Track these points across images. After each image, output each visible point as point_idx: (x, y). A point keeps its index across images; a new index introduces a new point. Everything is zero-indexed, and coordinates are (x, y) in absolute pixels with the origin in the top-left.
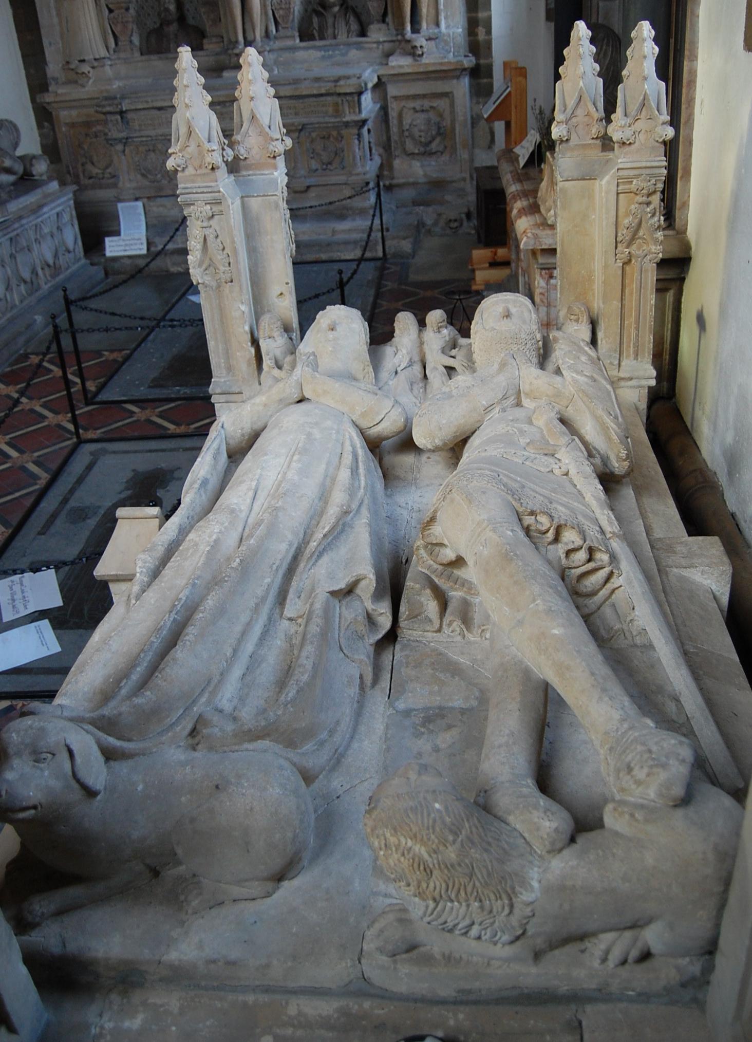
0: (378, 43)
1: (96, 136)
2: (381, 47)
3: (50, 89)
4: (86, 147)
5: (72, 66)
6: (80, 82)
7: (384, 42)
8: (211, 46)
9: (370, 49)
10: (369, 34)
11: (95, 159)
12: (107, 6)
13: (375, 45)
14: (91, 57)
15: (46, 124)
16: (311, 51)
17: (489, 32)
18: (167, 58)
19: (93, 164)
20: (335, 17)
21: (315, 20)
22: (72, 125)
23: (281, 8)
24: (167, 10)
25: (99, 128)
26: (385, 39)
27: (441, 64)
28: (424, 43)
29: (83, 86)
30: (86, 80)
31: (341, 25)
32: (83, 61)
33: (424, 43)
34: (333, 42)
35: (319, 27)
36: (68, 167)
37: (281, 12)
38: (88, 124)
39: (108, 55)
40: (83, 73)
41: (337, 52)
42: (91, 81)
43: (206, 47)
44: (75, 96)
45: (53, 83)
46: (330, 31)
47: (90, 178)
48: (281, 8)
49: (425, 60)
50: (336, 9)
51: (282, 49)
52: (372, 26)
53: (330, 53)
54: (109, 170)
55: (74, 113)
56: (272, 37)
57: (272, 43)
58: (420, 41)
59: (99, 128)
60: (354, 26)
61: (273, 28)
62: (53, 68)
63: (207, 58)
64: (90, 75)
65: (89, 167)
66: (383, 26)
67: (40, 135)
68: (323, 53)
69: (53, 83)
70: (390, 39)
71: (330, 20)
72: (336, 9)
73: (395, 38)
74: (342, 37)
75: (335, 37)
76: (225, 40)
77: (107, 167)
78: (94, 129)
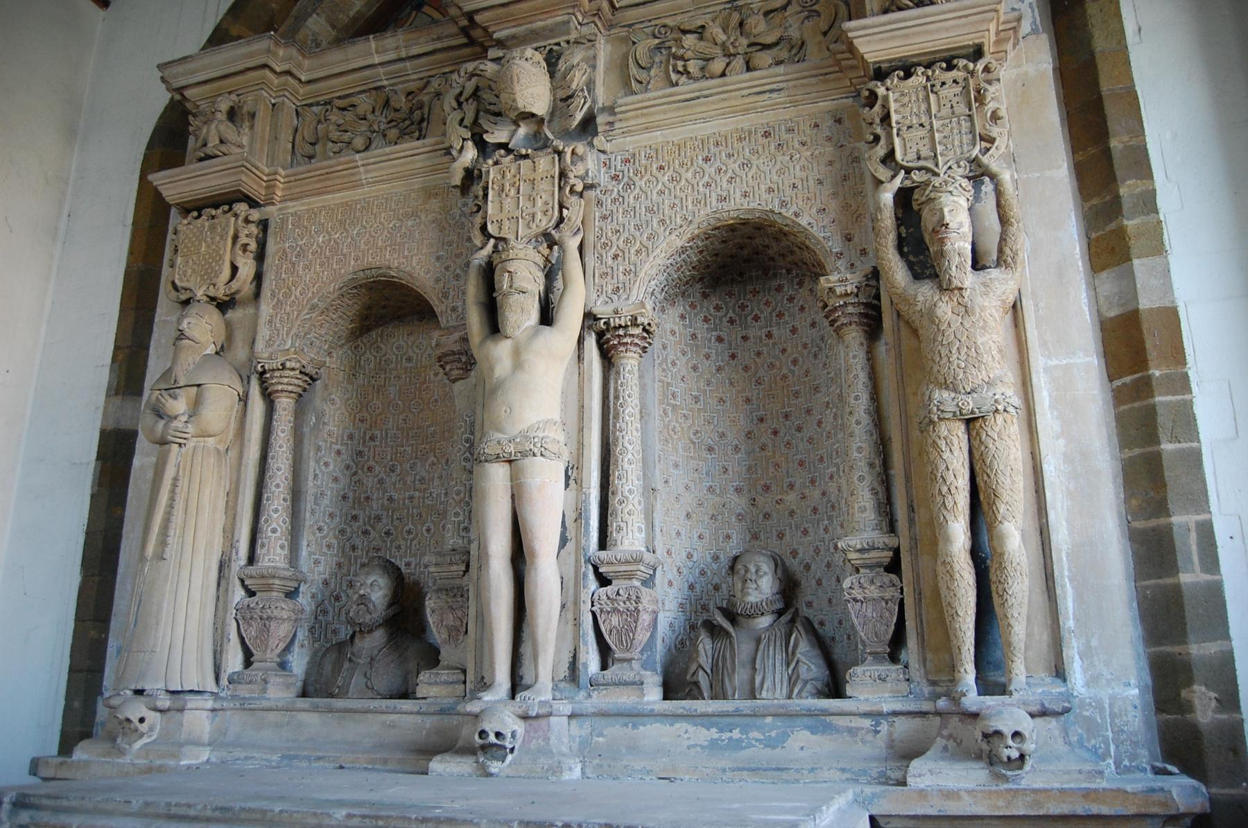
0: (876, 715)
2: (884, 727)
7: (895, 714)
8: (433, 691)
9: (852, 732)
10: (849, 690)
12: (242, 581)
13: (867, 723)
14: (161, 685)
16: (681, 726)
17: (1229, 699)
18: (331, 710)
20: (758, 641)
21: (705, 645)
23: (615, 610)
24: (363, 600)
26: (898, 707)
27: (1087, 794)
28: (1027, 725)
31: (773, 660)
33: (1027, 725)
34: (746, 705)
35: (714, 666)
37: (615, 620)
39: (211, 686)
41: (755, 734)
43: (421, 691)
46: (740, 677)
48: (615, 610)
49: (1030, 778)
50: (764, 622)
51: (603, 714)
52: (859, 670)
53: (736, 734)
56: (583, 680)
57: (583, 694)
58: (1008, 714)
60: (811, 667)
61: (591, 660)
63: (419, 719)
66: (893, 670)
68: (714, 733)
70: (912, 707)
71: (744, 648)
72: (764, 622)
73: (926, 706)
74: (773, 694)
75: (753, 696)
76: (470, 676)
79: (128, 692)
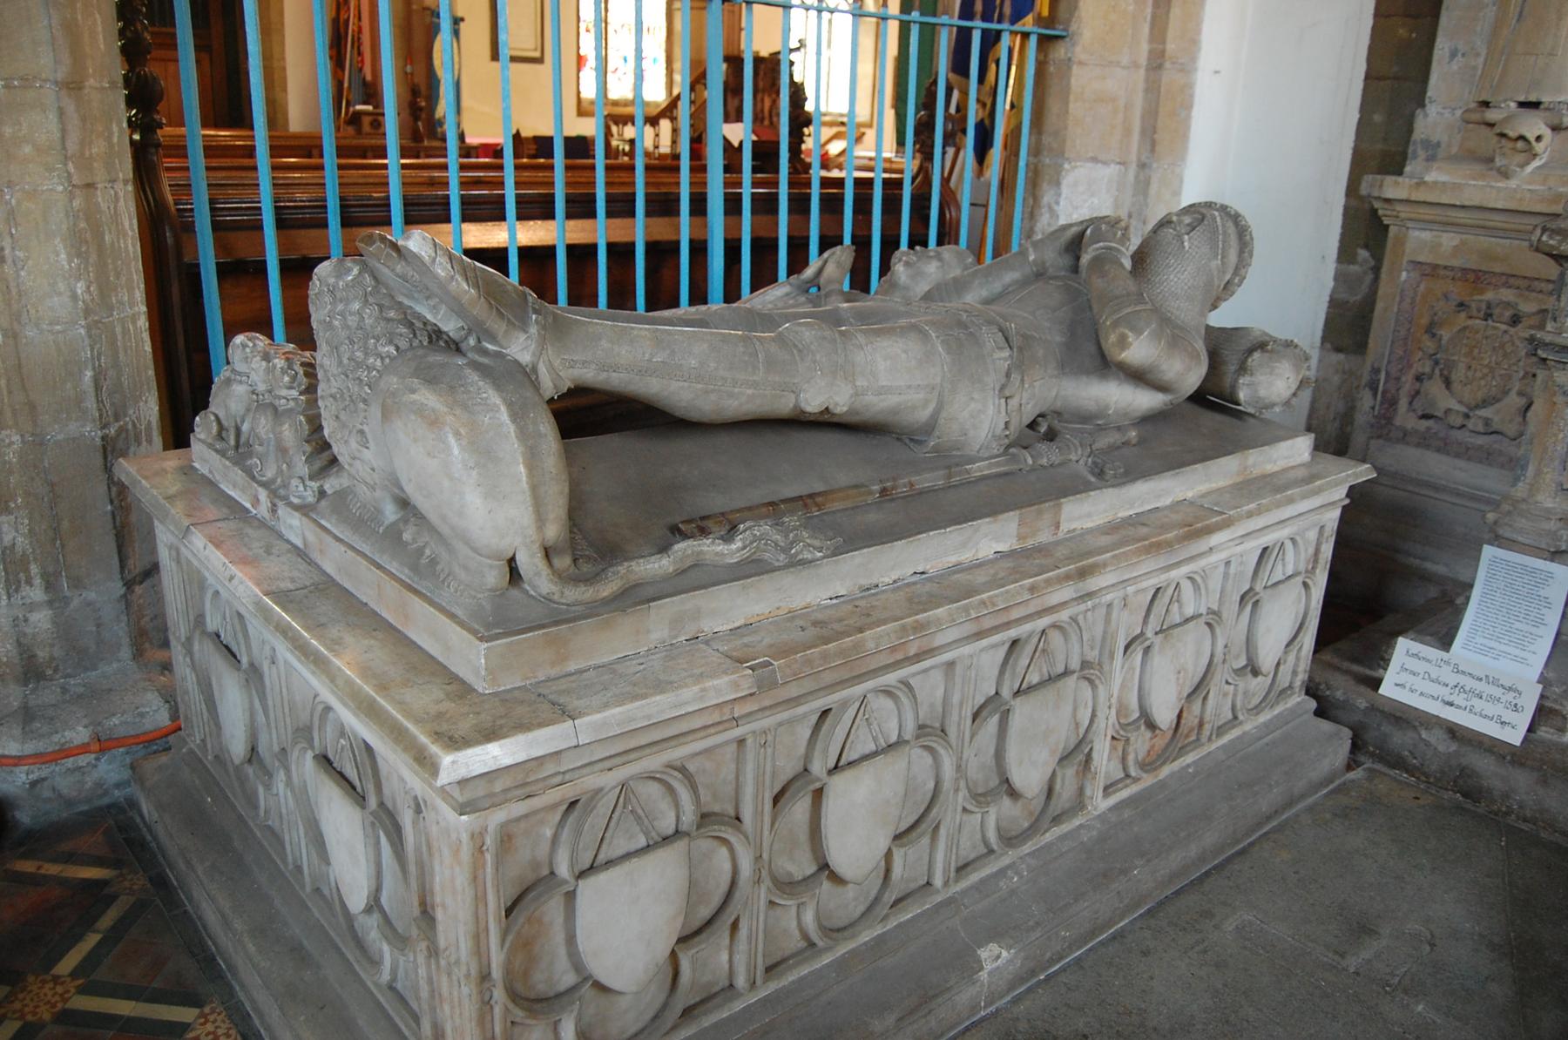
1: (1488, 316)
3: (1408, 169)
4: (1445, 334)
5: (1492, 115)
6: (1499, 162)
11: (1458, 374)
15: (1363, 254)
19: (1448, 383)
22: (1431, 271)
25: (1507, 295)
29: (1505, 174)
30: (1521, 158)
32: (1535, 105)
36: (1376, 371)
38: (1475, 278)
40: (1522, 138)
42: (1536, 163)
44: (1471, 197)
45: (1422, 154)
47: (1425, 417)
54: (1483, 413)
55: (1449, 240)
59: (1507, 295)
62: (1437, 117)
64: (1539, 147)
65: (1435, 388)
67: (1339, 277)
69: (1422, 154)
77: (1485, 403)
78: (1489, 295)
79: (1513, 105)
